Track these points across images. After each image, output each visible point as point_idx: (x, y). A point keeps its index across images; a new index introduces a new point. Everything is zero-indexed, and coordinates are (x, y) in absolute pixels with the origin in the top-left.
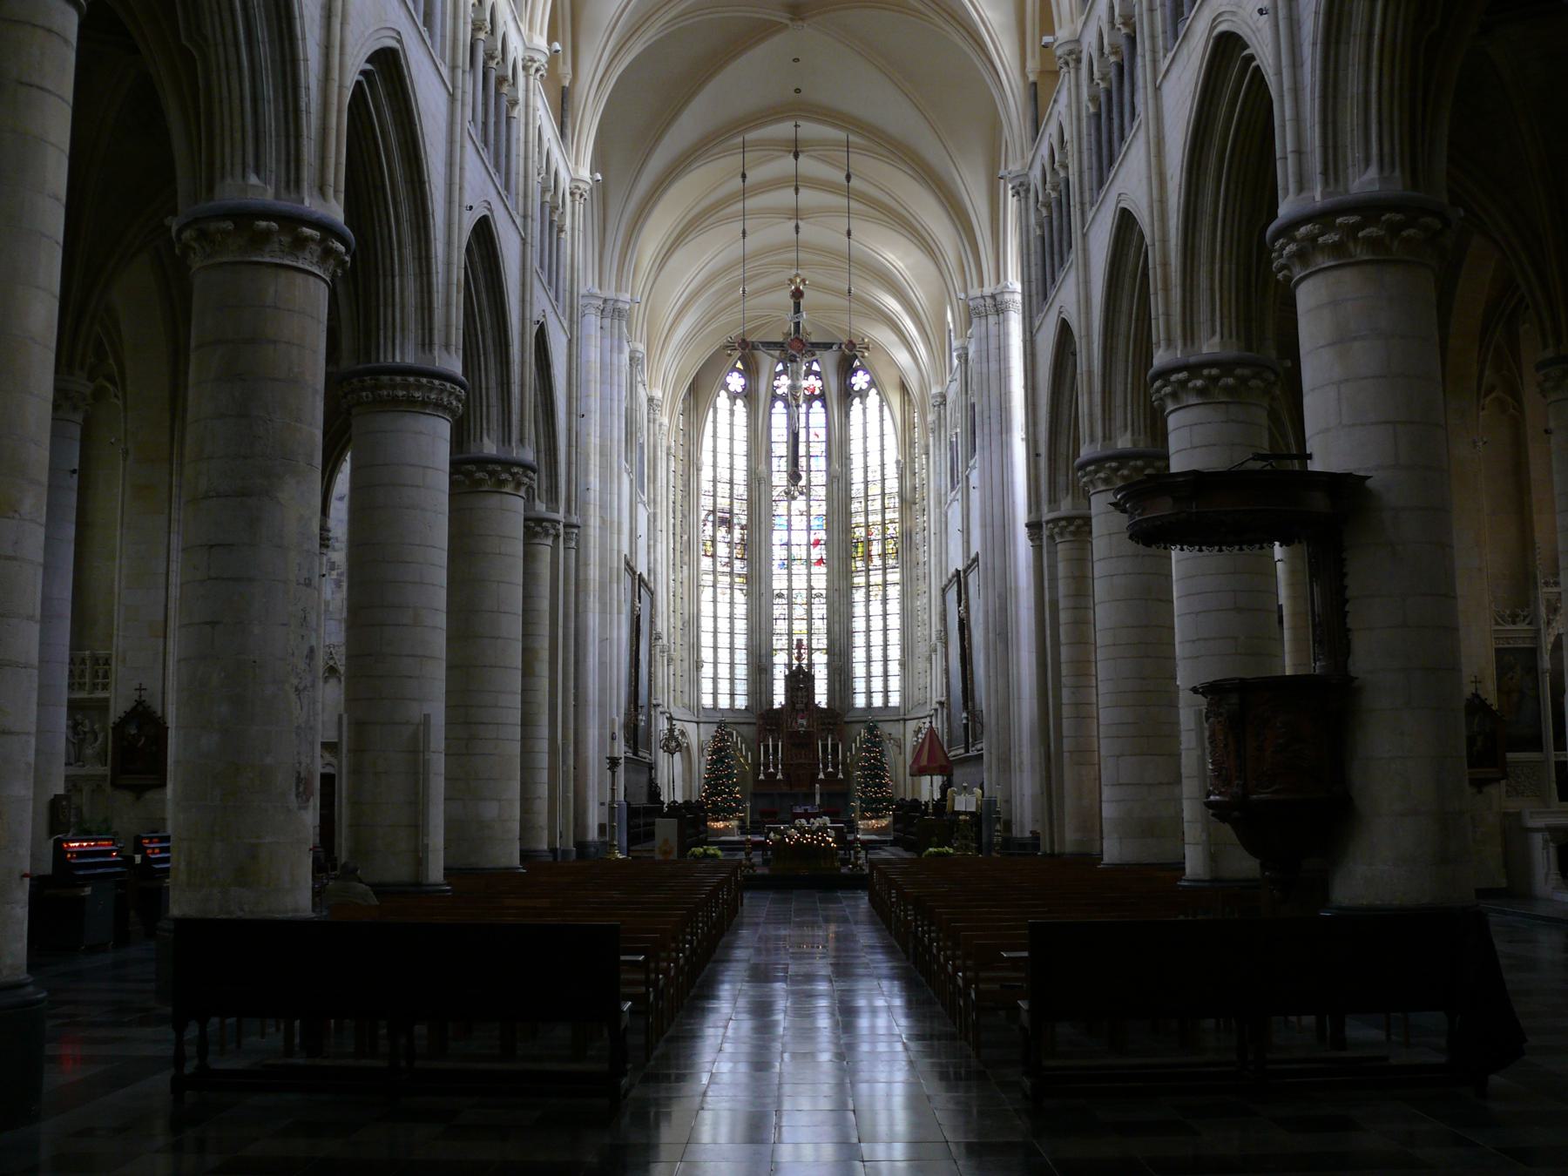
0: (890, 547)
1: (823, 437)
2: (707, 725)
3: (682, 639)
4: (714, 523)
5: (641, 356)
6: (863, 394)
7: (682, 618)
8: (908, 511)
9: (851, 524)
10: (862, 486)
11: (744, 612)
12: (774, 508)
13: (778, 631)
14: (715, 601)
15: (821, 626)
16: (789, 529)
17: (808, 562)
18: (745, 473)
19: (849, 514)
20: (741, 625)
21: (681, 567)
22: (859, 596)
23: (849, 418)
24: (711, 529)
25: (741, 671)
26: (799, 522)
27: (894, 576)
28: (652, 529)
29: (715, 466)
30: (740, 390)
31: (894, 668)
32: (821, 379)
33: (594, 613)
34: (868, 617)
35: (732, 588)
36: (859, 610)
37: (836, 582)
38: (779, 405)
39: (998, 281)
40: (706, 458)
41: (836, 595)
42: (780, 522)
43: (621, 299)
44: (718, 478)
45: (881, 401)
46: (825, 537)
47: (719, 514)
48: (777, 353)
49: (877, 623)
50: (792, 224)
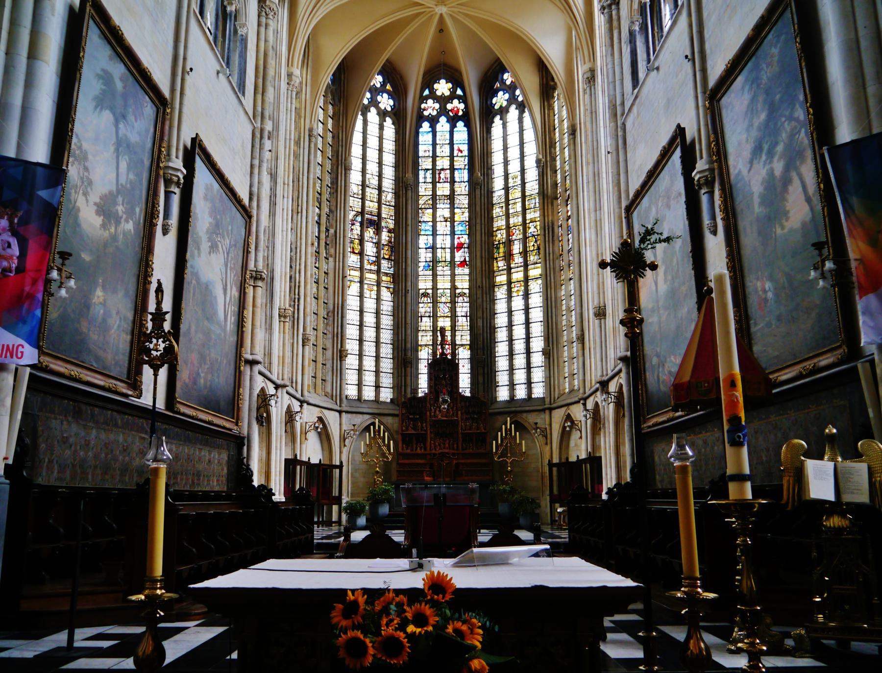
0: (531, 244)
1: (466, 153)
2: (349, 415)
6: (503, 111)
8: (550, 207)
9: (493, 228)
10: (503, 192)
11: (390, 309)
12: (420, 215)
13: (423, 328)
14: (361, 296)
16: (434, 234)
17: (452, 264)
18: (394, 182)
19: (491, 219)
20: (387, 321)
22: (501, 293)
24: (359, 228)
25: (387, 365)
26: (443, 228)
29: (364, 171)
30: (389, 109)
31: (538, 359)
34: (510, 312)
36: (501, 306)
37: (479, 280)
38: (426, 126)
40: (356, 164)
41: (479, 292)
42: (426, 228)
44: (367, 183)
46: (467, 241)
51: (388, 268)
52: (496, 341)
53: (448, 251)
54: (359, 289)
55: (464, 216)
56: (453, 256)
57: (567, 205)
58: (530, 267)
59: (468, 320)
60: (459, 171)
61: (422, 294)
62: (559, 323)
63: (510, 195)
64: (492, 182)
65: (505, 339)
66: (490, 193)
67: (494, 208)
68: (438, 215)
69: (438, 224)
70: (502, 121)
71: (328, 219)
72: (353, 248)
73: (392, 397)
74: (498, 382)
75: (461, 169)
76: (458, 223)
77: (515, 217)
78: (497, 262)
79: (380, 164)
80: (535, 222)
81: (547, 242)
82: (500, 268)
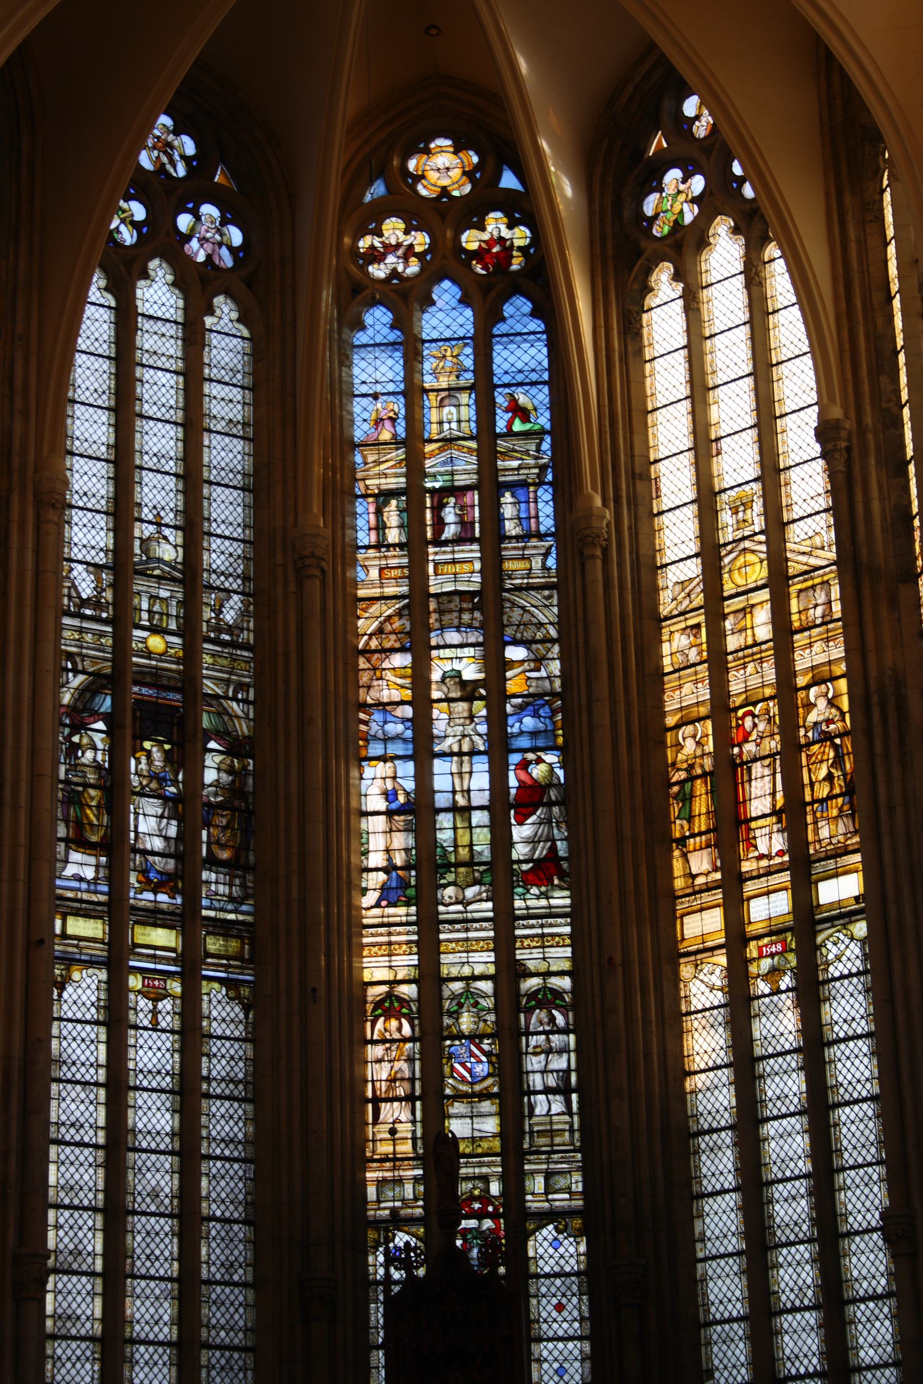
1: (544, 420)
8: (884, 612)
9: (663, 714)
10: (693, 568)
12: (364, 678)
13: (385, 1148)
15: (561, 1123)
23: (638, 335)
51: (231, 899)
53: (479, 817)
60: (520, 492)
61: (378, 1004)
63: (726, 576)
64: (653, 532)
67: (664, 638)
68: (436, 676)
69: (439, 713)
70: (680, 286)
75: (524, 484)
77: (751, 666)
78: (684, 856)
80: (833, 679)
82: (700, 880)
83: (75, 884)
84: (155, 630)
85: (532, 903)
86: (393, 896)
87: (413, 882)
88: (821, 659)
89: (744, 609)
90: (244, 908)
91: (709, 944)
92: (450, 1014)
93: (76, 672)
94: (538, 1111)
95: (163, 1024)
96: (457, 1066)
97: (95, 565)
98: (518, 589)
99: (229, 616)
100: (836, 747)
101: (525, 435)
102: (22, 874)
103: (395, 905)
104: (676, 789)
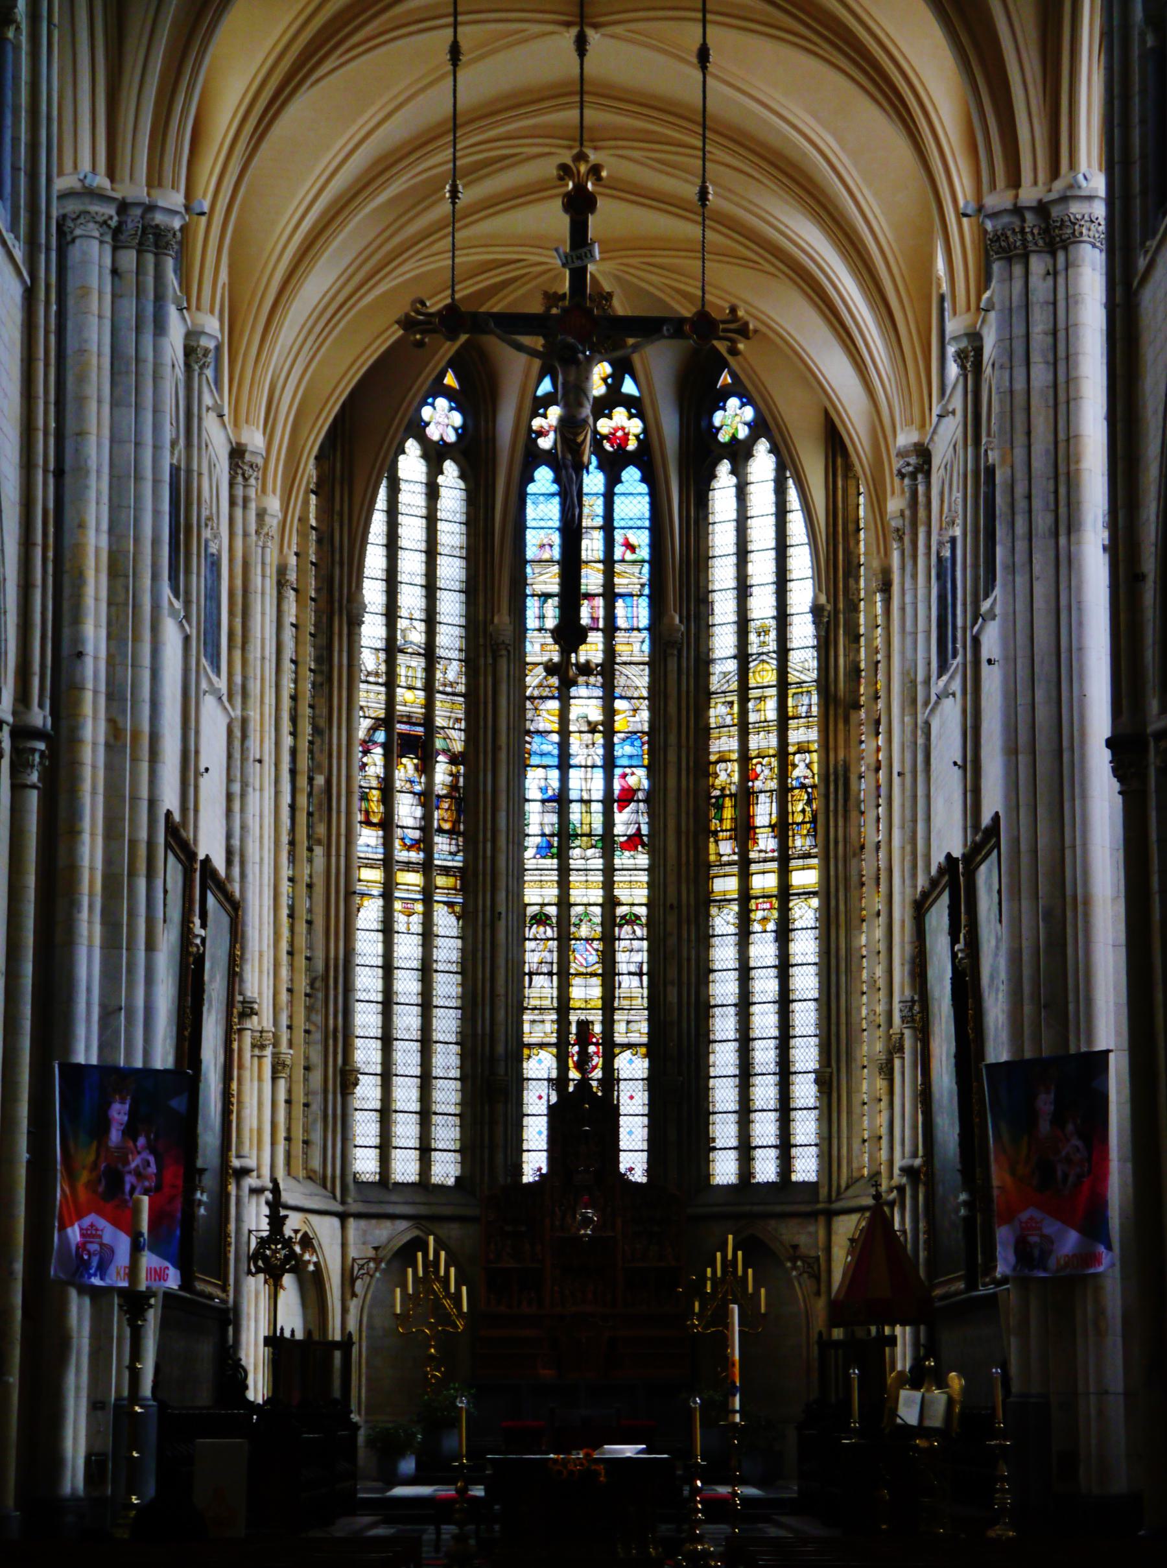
0: (798, 807)
1: (644, 553)
2: (363, 1223)
3: (308, 1019)
4: (387, 747)
5: (211, 345)
6: (739, 453)
7: (309, 969)
8: (841, 726)
9: (709, 753)
10: (732, 666)
11: (455, 956)
12: (529, 715)
14: (387, 930)
15: (637, 992)
16: (564, 764)
17: (608, 843)
18: (463, 632)
19: (703, 733)
20: (447, 987)
21: (310, 849)
22: (724, 922)
25: (447, 1096)
27: (805, 877)
28: (237, 755)
29: (391, 613)
30: (451, 437)
31: (805, 1091)
32: (641, 416)
33: (90, 947)
34: (745, 972)
35: (428, 899)
36: (724, 954)
37: (672, 890)
38: (544, 477)
39: (1055, 173)
41: (672, 919)
43: (161, 203)
44: (400, 641)
45: (781, 469)
46: (645, 784)
47: (401, 728)
48: (538, 342)
49: (765, 986)
50: (574, 31)
51: (451, 853)
52: (712, 1037)
53: (597, 807)
54: (381, 914)
55: (637, 719)
56: (609, 823)
57: (878, 734)
58: (794, 863)
59: (645, 983)
60: (628, 599)
61: (533, 917)
62: (854, 1012)
63: (751, 675)
64: (709, 636)
65: (732, 1035)
66: (703, 662)
69: (574, 739)
71: (311, 751)
72: (367, 813)
73: (458, 1173)
74: (714, 1140)
75: (632, 595)
76: (622, 735)
77: (762, 734)
78: (716, 842)
79: (431, 588)
80: (809, 752)
81: (831, 814)
82: (725, 859)
83: (365, 849)
84: (410, 688)
85: (625, 861)
86: (544, 852)
87: (556, 844)
88: (803, 738)
89: (760, 698)
90: (457, 858)
91: (728, 897)
92: (575, 925)
93: (365, 717)
94: (623, 985)
95: (412, 930)
96: (578, 956)
97: (377, 649)
98: (625, 663)
99: (451, 676)
100: (807, 792)
101: (634, 562)
102: (343, 852)
103: (544, 857)
104: (713, 800)
